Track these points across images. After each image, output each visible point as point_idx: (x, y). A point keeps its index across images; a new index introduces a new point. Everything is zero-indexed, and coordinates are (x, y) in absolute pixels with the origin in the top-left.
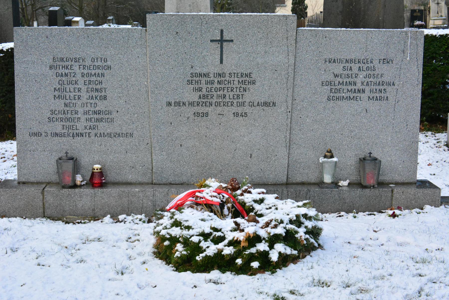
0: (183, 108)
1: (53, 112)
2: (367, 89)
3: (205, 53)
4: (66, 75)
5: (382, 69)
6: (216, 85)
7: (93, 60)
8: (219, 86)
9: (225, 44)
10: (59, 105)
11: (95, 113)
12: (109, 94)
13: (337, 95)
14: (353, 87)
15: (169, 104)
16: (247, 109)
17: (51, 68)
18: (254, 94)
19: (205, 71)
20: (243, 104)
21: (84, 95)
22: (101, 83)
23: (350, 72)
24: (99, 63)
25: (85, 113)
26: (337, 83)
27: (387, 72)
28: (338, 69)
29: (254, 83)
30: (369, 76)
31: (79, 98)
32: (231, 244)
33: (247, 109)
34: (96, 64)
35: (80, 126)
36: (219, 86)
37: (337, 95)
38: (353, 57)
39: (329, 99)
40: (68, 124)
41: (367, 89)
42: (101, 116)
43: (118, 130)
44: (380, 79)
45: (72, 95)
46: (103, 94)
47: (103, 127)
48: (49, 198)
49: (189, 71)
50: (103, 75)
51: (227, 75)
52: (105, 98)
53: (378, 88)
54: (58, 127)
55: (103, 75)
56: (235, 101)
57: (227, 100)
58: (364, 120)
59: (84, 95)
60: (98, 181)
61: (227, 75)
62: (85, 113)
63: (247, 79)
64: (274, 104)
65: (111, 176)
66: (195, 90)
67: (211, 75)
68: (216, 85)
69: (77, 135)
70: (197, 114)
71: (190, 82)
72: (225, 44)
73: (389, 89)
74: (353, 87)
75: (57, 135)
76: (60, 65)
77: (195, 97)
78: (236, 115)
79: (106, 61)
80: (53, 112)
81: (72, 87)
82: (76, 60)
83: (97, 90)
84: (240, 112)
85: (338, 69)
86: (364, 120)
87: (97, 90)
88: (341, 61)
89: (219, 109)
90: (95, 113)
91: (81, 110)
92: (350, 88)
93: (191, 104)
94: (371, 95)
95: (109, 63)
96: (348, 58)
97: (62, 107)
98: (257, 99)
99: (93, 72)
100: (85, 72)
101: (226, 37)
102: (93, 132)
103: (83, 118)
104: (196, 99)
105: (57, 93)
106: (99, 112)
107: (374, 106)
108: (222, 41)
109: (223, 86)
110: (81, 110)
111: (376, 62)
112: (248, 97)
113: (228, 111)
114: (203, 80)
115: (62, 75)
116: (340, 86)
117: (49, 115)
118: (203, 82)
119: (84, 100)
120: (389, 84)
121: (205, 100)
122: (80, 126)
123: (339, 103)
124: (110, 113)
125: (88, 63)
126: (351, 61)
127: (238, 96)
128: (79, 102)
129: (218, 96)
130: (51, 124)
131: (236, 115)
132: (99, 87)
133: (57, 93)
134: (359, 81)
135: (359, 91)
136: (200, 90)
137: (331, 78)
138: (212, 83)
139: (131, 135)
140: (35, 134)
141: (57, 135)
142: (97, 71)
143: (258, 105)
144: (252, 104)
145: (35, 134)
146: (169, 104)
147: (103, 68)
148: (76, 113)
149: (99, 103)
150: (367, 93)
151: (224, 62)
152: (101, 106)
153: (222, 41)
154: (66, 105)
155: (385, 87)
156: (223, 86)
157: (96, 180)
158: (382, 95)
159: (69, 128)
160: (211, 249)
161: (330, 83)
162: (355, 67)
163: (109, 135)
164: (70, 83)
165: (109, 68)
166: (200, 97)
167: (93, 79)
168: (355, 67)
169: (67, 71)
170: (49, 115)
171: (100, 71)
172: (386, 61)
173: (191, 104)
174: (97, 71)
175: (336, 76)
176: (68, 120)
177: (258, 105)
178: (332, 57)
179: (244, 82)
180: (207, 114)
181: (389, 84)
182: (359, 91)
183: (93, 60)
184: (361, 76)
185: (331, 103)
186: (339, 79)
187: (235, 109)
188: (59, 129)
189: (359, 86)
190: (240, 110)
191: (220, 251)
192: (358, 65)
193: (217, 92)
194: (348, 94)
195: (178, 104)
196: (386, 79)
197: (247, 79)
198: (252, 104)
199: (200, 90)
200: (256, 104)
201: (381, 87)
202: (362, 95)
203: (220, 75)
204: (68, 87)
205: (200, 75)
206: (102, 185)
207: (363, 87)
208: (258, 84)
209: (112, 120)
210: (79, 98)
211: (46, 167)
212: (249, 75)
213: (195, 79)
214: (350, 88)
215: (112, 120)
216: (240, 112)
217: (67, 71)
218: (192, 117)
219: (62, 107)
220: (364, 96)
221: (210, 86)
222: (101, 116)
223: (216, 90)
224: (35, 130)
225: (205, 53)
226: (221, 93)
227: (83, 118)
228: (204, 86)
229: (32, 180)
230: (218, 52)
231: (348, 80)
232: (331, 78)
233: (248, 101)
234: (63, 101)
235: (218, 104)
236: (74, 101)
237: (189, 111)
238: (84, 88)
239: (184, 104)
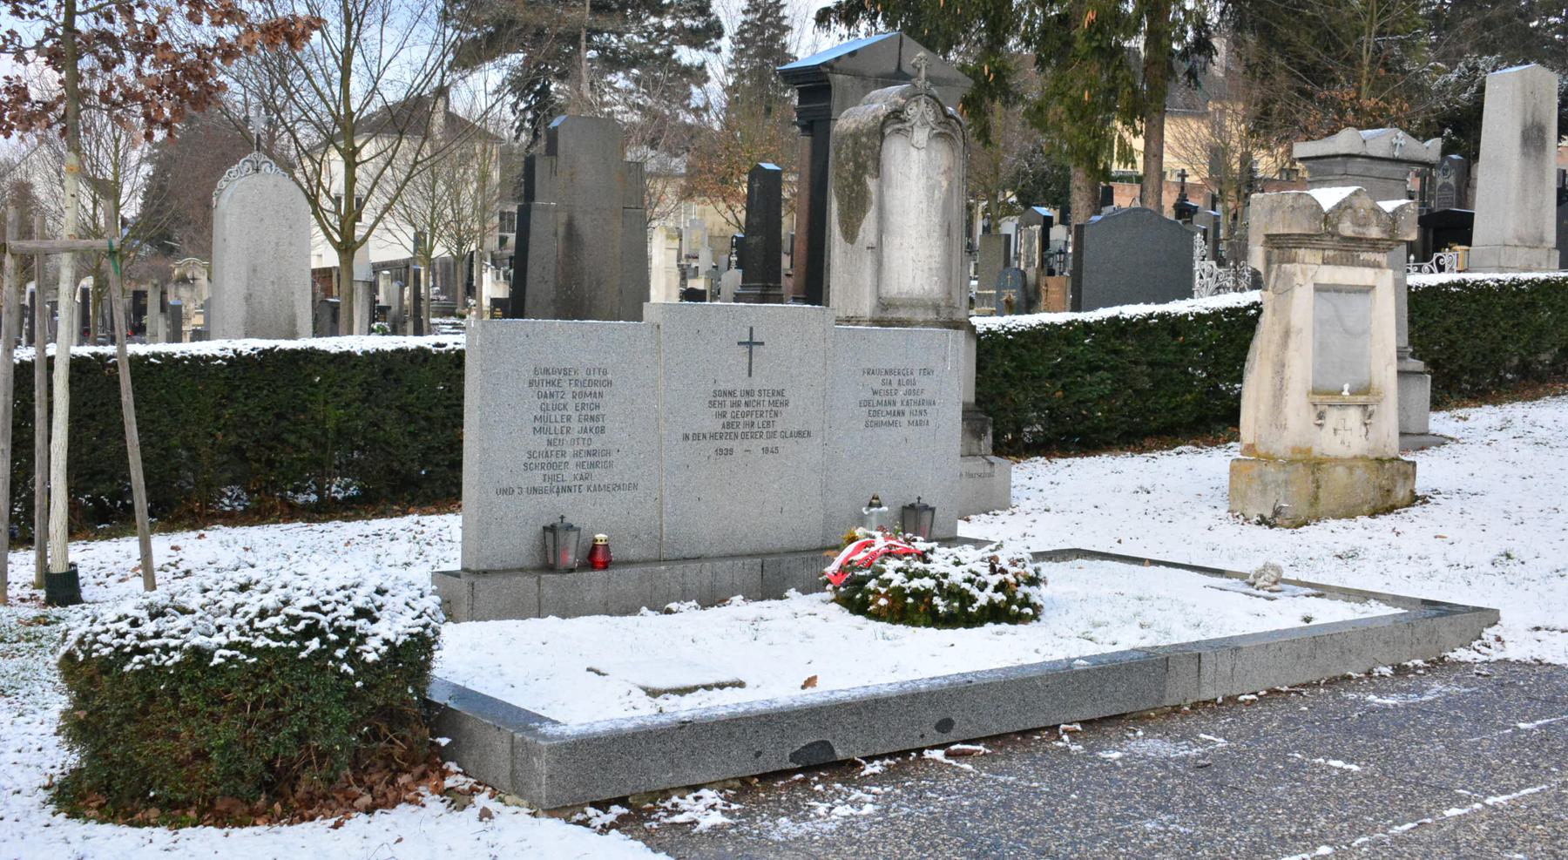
0: (703, 442)
1: (531, 454)
2: (907, 410)
4: (552, 395)
5: (923, 382)
6: (743, 408)
11: (588, 453)
12: (608, 424)
16: (778, 442)
17: (531, 384)
19: (730, 387)
20: (772, 435)
21: (576, 426)
22: (598, 407)
24: (597, 377)
25: (576, 454)
27: (927, 386)
28: (876, 382)
30: (908, 393)
32: (996, 590)
35: (569, 475)
40: (551, 472)
41: (907, 410)
45: (558, 426)
46: (600, 424)
47: (600, 476)
48: (548, 591)
52: (603, 430)
54: (537, 478)
59: (576, 426)
60: (595, 559)
62: (576, 454)
65: (615, 554)
68: (743, 408)
69: (564, 490)
70: (719, 451)
71: (712, 404)
75: (535, 490)
76: (546, 381)
77: (716, 426)
78: (765, 450)
79: (605, 373)
80: (531, 454)
81: (558, 414)
82: (566, 372)
85: (876, 382)
87: (592, 418)
90: (588, 453)
91: (569, 450)
92: (889, 408)
93: (713, 436)
96: (888, 367)
100: (577, 390)
103: (573, 462)
104: (719, 429)
108: (751, 344)
110: (569, 450)
113: (757, 445)
114: (729, 400)
117: (525, 459)
122: (569, 475)
123: (878, 430)
125: (582, 375)
128: (568, 438)
129: (746, 424)
130: (529, 474)
131: (765, 450)
132: (595, 413)
134: (898, 399)
136: (724, 415)
137: (869, 395)
138: (738, 404)
139: (635, 486)
141: (535, 490)
142: (597, 389)
146: (686, 437)
147: (602, 384)
152: (596, 444)
153: (751, 344)
154: (549, 443)
157: (600, 557)
159: (553, 478)
160: (982, 598)
161: (867, 403)
163: (606, 488)
164: (556, 408)
165: (610, 383)
167: (588, 400)
168: (895, 379)
169: (553, 389)
170: (525, 459)
171: (597, 389)
172: (927, 372)
173: (713, 436)
176: (551, 465)
179: (775, 403)
180: (730, 452)
185: (869, 432)
186: (877, 397)
187: (764, 443)
189: (899, 407)
190: (769, 443)
191: (991, 600)
193: (745, 417)
195: (697, 437)
196: (925, 396)
198: (784, 435)
199: (724, 415)
206: (606, 565)
209: (611, 464)
211: (518, 544)
212: (781, 393)
214: (889, 408)
217: (553, 389)
220: (904, 420)
223: (745, 415)
224: (505, 486)
227: (573, 462)
228: (729, 409)
229: (498, 566)
235: (745, 436)
237: (710, 446)
238: (575, 416)
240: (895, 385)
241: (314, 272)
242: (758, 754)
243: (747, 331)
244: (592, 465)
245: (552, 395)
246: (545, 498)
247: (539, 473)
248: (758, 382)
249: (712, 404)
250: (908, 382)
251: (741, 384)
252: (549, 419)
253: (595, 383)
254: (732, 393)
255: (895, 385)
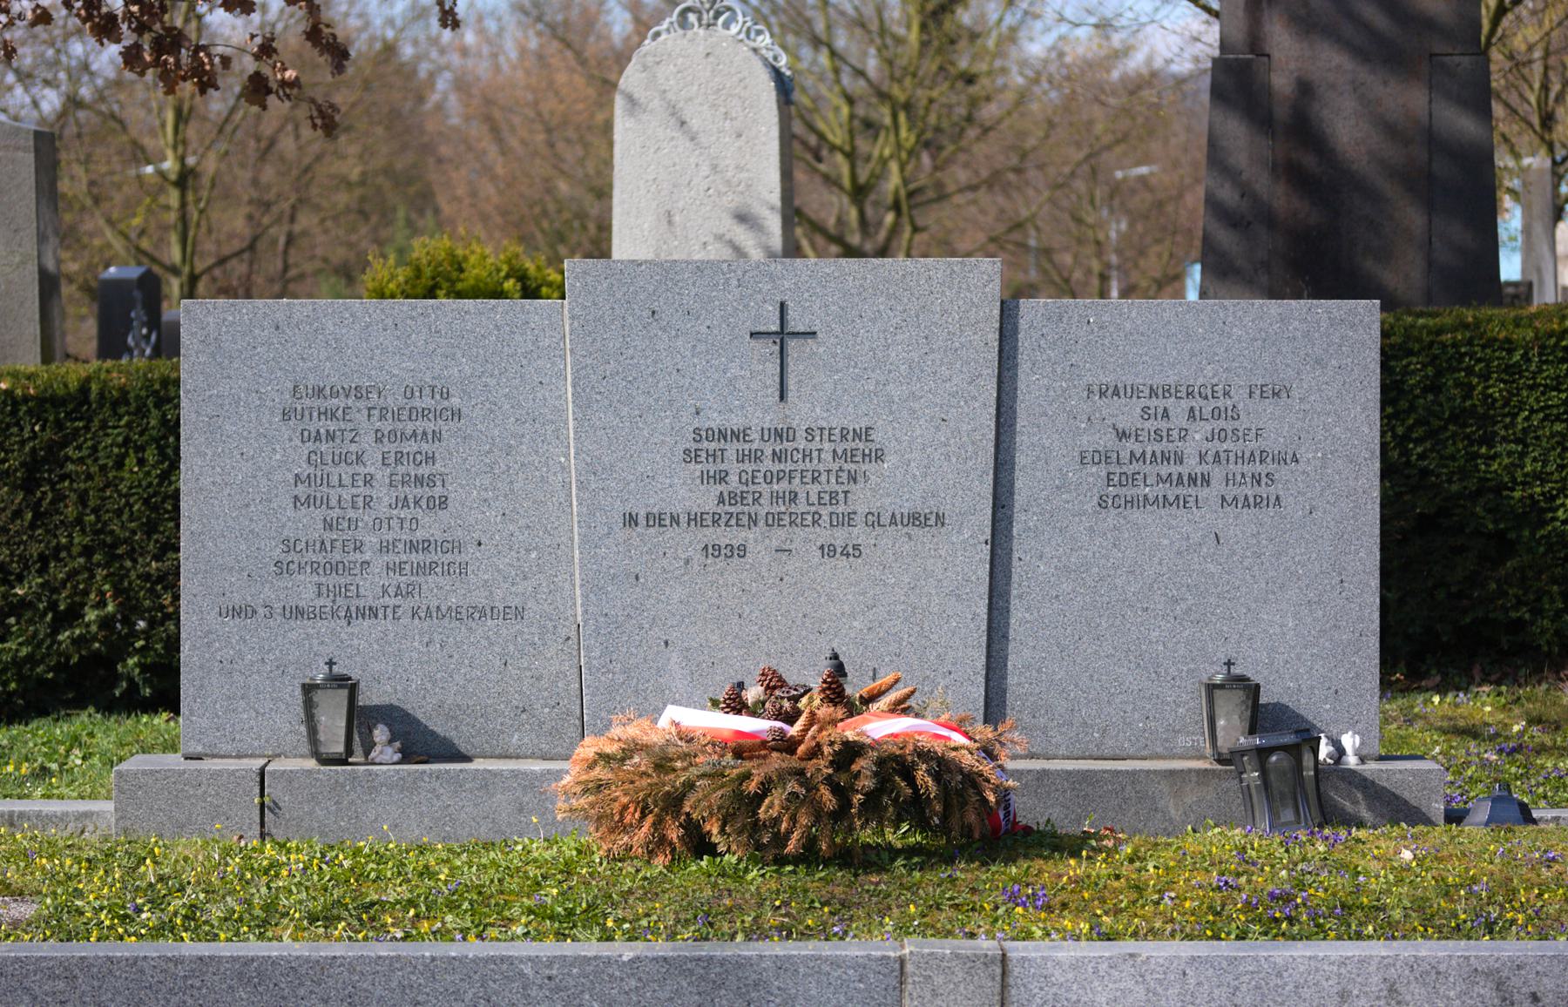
0: (671, 532)
1: (289, 545)
2: (1217, 473)
3: (734, 370)
4: (331, 436)
6: (768, 464)
7: (409, 393)
8: (776, 467)
9: (792, 344)
10: (309, 524)
11: (412, 547)
12: (454, 492)
13: (1129, 492)
14: (1175, 469)
15: (631, 520)
16: (859, 534)
17: (285, 415)
19: (736, 422)
20: (848, 520)
21: (383, 496)
22: (430, 459)
23: (1163, 425)
24: (427, 402)
25: (385, 548)
26: (1125, 455)
27: (1273, 425)
28: (1128, 414)
29: (879, 456)
30: (1221, 435)
31: (367, 505)
33: (859, 534)
34: (417, 403)
35: (370, 586)
36: (776, 467)
37: (1129, 492)
38: (1171, 380)
39: (1102, 503)
40: (333, 580)
41: (1217, 473)
43: (480, 598)
44: (1252, 445)
45: (346, 496)
46: (438, 491)
47: (435, 590)
49: (689, 423)
50: (437, 436)
51: (801, 434)
52: (444, 502)
53: (1248, 469)
54: (304, 590)
55: (437, 436)
56: (825, 512)
57: (802, 507)
58: (1211, 567)
59: (383, 496)
61: (801, 434)
62: (385, 548)
63: (859, 448)
66: (706, 478)
67: (755, 436)
68: (768, 464)
71: (691, 456)
72: (792, 344)
73: (1282, 473)
74: (1175, 469)
75: (299, 612)
77: (706, 499)
78: (828, 551)
81: (346, 471)
82: (359, 393)
83: (419, 481)
84: (839, 543)
85: (1128, 414)
86: (1211, 567)
87: (419, 481)
88: (1135, 392)
89: (778, 536)
90: (412, 547)
91: (371, 540)
92: (1164, 470)
93: (697, 520)
95: (455, 401)
96: (1157, 381)
99: (410, 428)
100: (387, 426)
101: (796, 323)
102: (407, 604)
104: (710, 505)
105: (301, 490)
106: (426, 545)
107: (1239, 526)
108: (783, 335)
109: (789, 466)
110: (371, 540)
111: (1239, 395)
112: (862, 500)
113: (806, 540)
114: (732, 448)
115: (318, 438)
116: (1135, 467)
117: (277, 553)
118: (731, 454)
119: (382, 510)
120: (1281, 460)
121: (736, 507)
122: (370, 586)
123: (1136, 515)
124: (457, 546)
125: (394, 400)
126: (1167, 391)
127: (833, 496)
129: (776, 497)
132: (424, 470)
133: (301, 490)
134: (1189, 450)
135: (1193, 480)
136: (722, 478)
137: (1107, 440)
138: (756, 457)
139: (519, 613)
140: (236, 612)
141: (299, 612)
142: (421, 425)
143: (893, 522)
144: (874, 521)
145: (236, 612)
146: (631, 520)
147: (438, 414)
148: (358, 548)
149: (425, 519)
150: (1217, 487)
151: (791, 395)
152: (431, 526)
153: (783, 335)
154: (328, 525)
155: (1271, 467)
156: (789, 466)
158: (1263, 491)
161: (1104, 457)
162: (1179, 409)
163: (456, 614)
164: (343, 459)
165: (457, 414)
166: (721, 501)
167: (410, 447)
168: (1179, 409)
169: (333, 426)
170: (277, 553)
173: (697, 520)
174: (421, 425)
175: (1123, 435)
176: (334, 568)
177: (893, 522)
178: (1109, 379)
179: (849, 456)
180: (742, 551)
181: (1281, 460)
182: (1193, 480)
183: (409, 393)
184: (1199, 432)
186: (1130, 445)
187: (823, 535)
188: (306, 596)
189: (1191, 465)
190: (840, 537)
192: (1185, 404)
194: (1161, 489)
195: (655, 520)
197: (859, 448)
198: (874, 521)
199: (722, 478)
200: (885, 519)
201: (1259, 468)
202: (1203, 493)
203: (779, 434)
204: (335, 471)
205: (722, 435)
207: (1205, 468)
208: (891, 461)
210: (367, 505)
212: (865, 434)
213: (708, 446)
214: (1164, 470)
215: (463, 570)
216: (839, 543)
217: (333, 426)
218: (699, 558)
221: (748, 467)
223: (769, 478)
224: (237, 599)
225: (734, 370)
226: (784, 485)
228: (733, 467)
230: (773, 368)
231: (1158, 448)
232: (1107, 440)
233: (862, 509)
234: (318, 514)
235: (774, 521)
236: (351, 514)
237: (688, 541)
238: (381, 475)
239: (675, 520)
240: (1179, 418)
241: (1201, 297)
243: (772, 311)
244: (421, 569)
245: (331, 436)
246: (322, 626)
247: (307, 580)
248: (803, 412)
249: (691, 456)
250: (1217, 414)
251: (760, 415)
252: (326, 480)
253: (424, 413)
254: (739, 435)
255: (1179, 418)
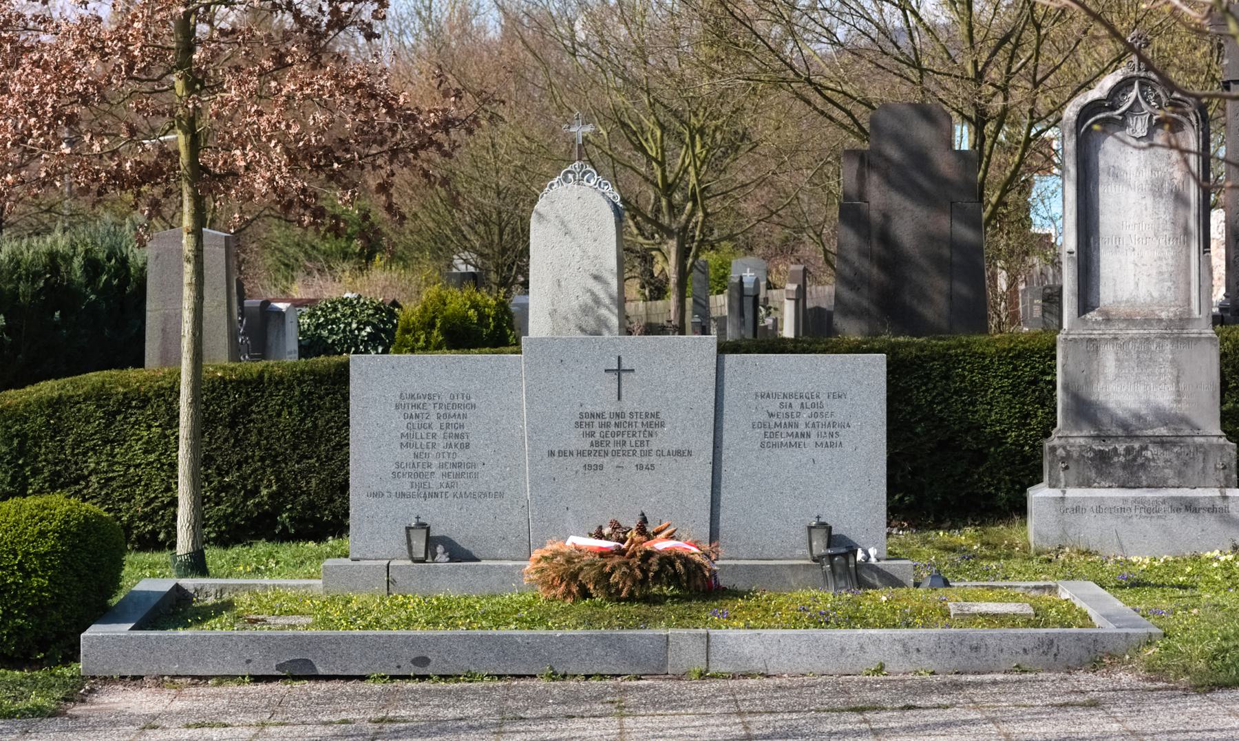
1: (399, 465)
2: (814, 432)
3: (598, 387)
6: (613, 429)
8: (616, 430)
9: (623, 375)
10: (407, 455)
11: (454, 465)
12: (473, 441)
13: (774, 440)
14: (795, 430)
15: (552, 453)
16: (653, 459)
17: (397, 407)
18: (663, 440)
19: (598, 410)
20: (649, 453)
21: (441, 442)
22: (462, 426)
23: (789, 410)
24: (460, 401)
25: (442, 466)
26: (772, 424)
27: (838, 410)
28: (774, 405)
29: (662, 425)
30: (815, 415)
31: (433, 447)
34: (456, 401)
35: (435, 482)
36: (616, 430)
37: (774, 440)
38: (793, 391)
39: (762, 446)
40: (418, 480)
42: (462, 470)
43: (484, 489)
44: (829, 419)
45: (424, 442)
46: (465, 440)
47: (463, 484)
49: (577, 410)
50: (465, 416)
51: (627, 415)
52: (468, 446)
53: (827, 430)
54: (405, 485)
55: (465, 416)
56: (638, 450)
57: (628, 448)
58: (811, 474)
59: (441, 442)
61: (627, 415)
62: (442, 466)
63: (653, 421)
64: (690, 453)
66: (585, 434)
67: (607, 416)
68: (613, 429)
69: (431, 495)
71: (578, 425)
72: (623, 375)
73: (843, 432)
74: (795, 430)
75: (403, 495)
76: (412, 404)
77: (585, 444)
78: (640, 467)
80: (399, 465)
82: (430, 397)
83: (457, 436)
84: (644, 464)
85: (774, 405)
86: (811, 474)
87: (457, 436)
88: (777, 396)
89: (617, 460)
90: (454, 465)
91: (435, 462)
94: (820, 440)
95: (473, 400)
96: (787, 391)
97: (411, 459)
98: (666, 446)
99: (453, 412)
100: (442, 412)
101: (625, 366)
102: (451, 491)
103: (439, 472)
104: (587, 447)
105: (404, 440)
106: (460, 465)
107: (824, 455)
109: (622, 429)
110: (435, 462)
111: (823, 397)
112: (655, 444)
114: (597, 421)
115: (411, 417)
116: (777, 429)
118: (596, 424)
119: (441, 449)
121: (599, 448)
122: (435, 482)
123: (777, 451)
124: (474, 465)
125: (446, 400)
126: (791, 396)
127: (642, 442)
129: (616, 443)
130: (397, 481)
132: (459, 431)
133: (404, 440)
135: (802, 435)
136: (592, 434)
137: (765, 417)
138: (607, 425)
139: (502, 495)
140: (375, 495)
141: (403, 495)
142: (457, 411)
143: (669, 454)
144: (660, 453)
145: (375, 495)
146: (552, 453)
147: (465, 407)
149: (460, 454)
150: (814, 437)
151: (623, 397)
152: (462, 457)
153: (619, 371)
154: (416, 456)
155: (838, 429)
156: (622, 429)
158: (834, 440)
162: (796, 404)
163: (473, 495)
164: (422, 426)
165: (474, 406)
166: (592, 445)
168: (796, 404)
169: (418, 412)
171: (461, 412)
173: (581, 453)
174: (457, 411)
175: (771, 415)
176: (419, 475)
177: (669, 454)
178: (765, 390)
179: (650, 425)
182: (802, 435)
184: (806, 414)
185: (766, 452)
186: (775, 419)
187: (637, 460)
188: (406, 488)
189: (802, 429)
190: (645, 461)
192: (799, 401)
194: (789, 439)
195: (563, 453)
196: (839, 418)
197: (653, 421)
198: (660, 453)
199: (592, 434)
200: (665, 453)
201: (832, 430)
202: (807, 441)
203: (618, 415)
204: (419, 432)
205: (593, 415)
207: (808, 430)
210: (433, 447)
213: (585, 420)
216: (644, 464)
217: (418, 412)
218: (582, 470)
219: (411, 459)
221: (604, 430)
222: (462, 470)
224: (375, 489)
225: (598, 387)
226: (620, 438)
227: (439, 472)
228: (597, 429)
231: (787, 421)
232: (765, 417)
233: (655, 449)
234: (412, 451)
235: (616, 454)
236: (426, 451)
237: (577, 463)
238: (440, 433)
239: (571, 453)
242: (248, 661)
244: (458, 476)
247: (406, 481)
248: (628, 405)
249: (578, 425)
250: (813, 405)
251: (610, 407)
253: (459, 406)
